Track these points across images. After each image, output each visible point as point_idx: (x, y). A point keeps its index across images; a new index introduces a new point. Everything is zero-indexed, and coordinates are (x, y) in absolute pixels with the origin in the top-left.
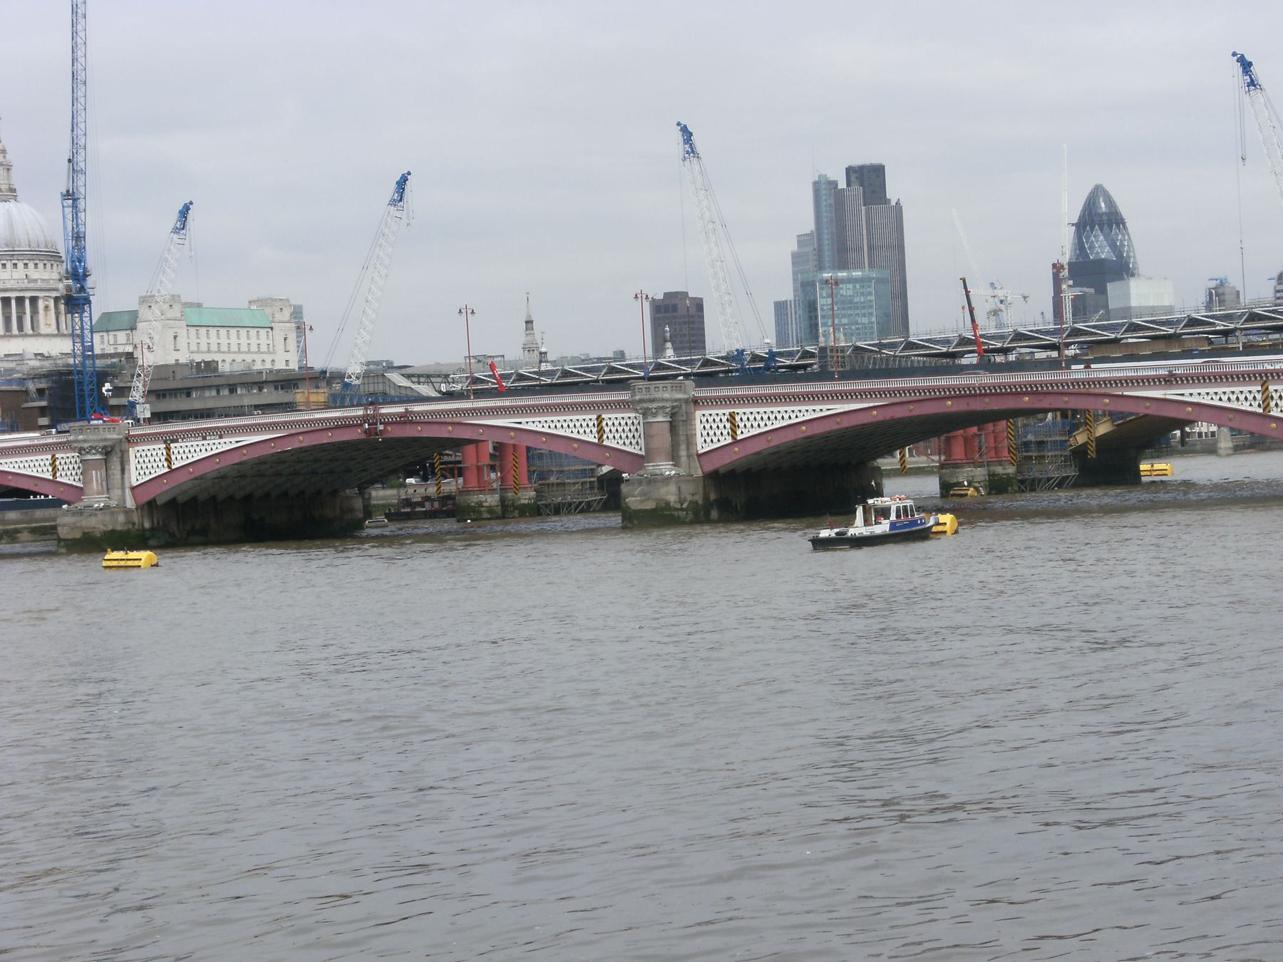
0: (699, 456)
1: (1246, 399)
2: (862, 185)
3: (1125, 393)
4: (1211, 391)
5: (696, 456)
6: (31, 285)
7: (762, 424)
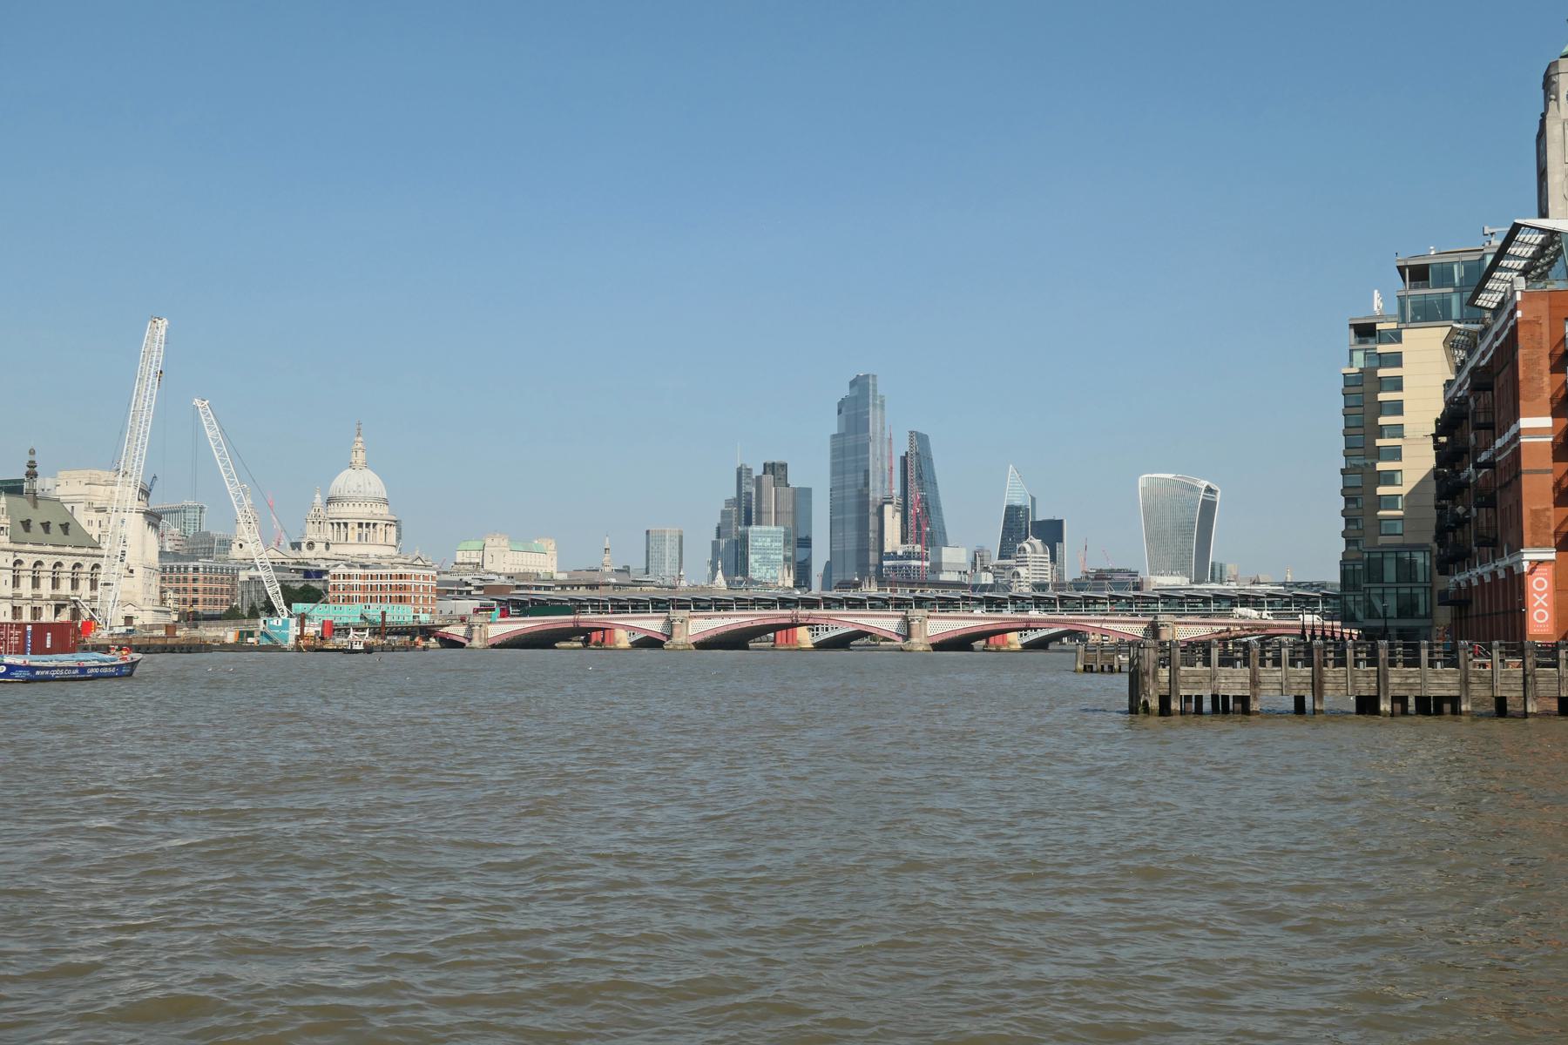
2: (773, 474)
6: (375, 517)
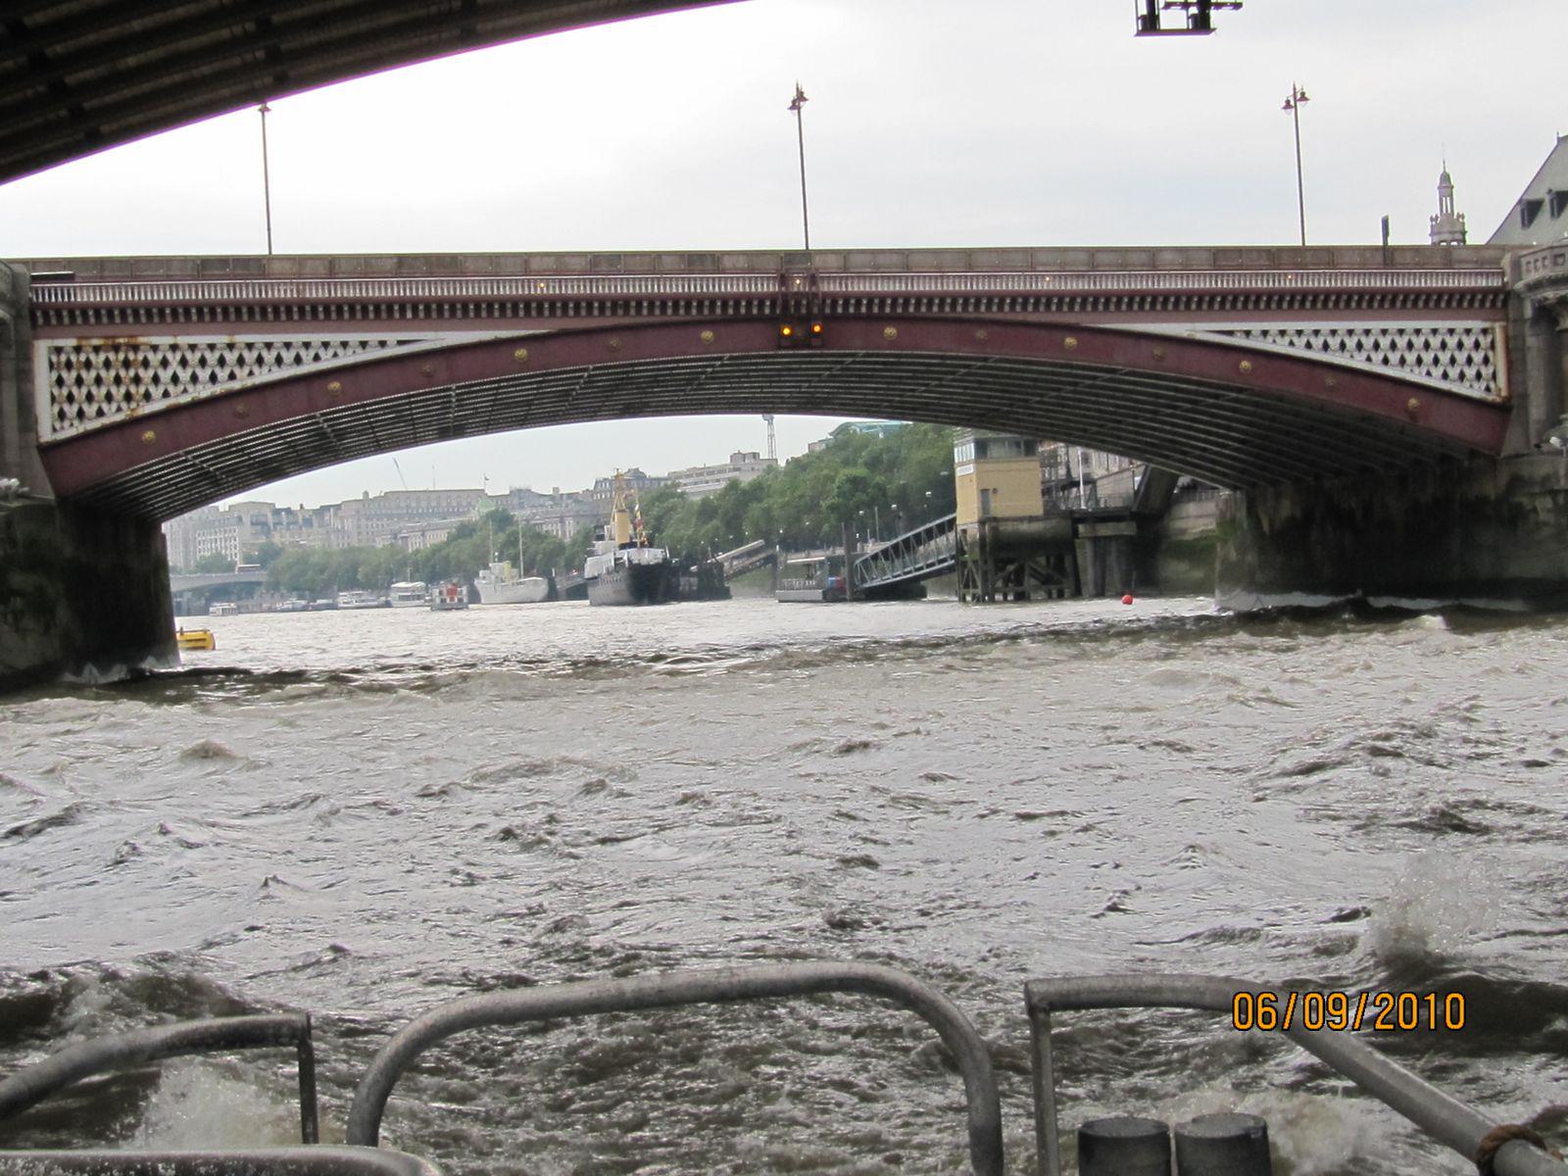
0: (48, 450)
1: (1360, 346)
3: (1102, 326)
4: (1291, 326)
5: (35, 454)
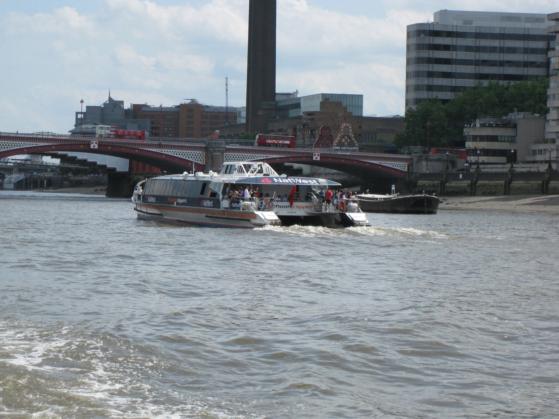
4: (171, 151)
7: (9, 147)
